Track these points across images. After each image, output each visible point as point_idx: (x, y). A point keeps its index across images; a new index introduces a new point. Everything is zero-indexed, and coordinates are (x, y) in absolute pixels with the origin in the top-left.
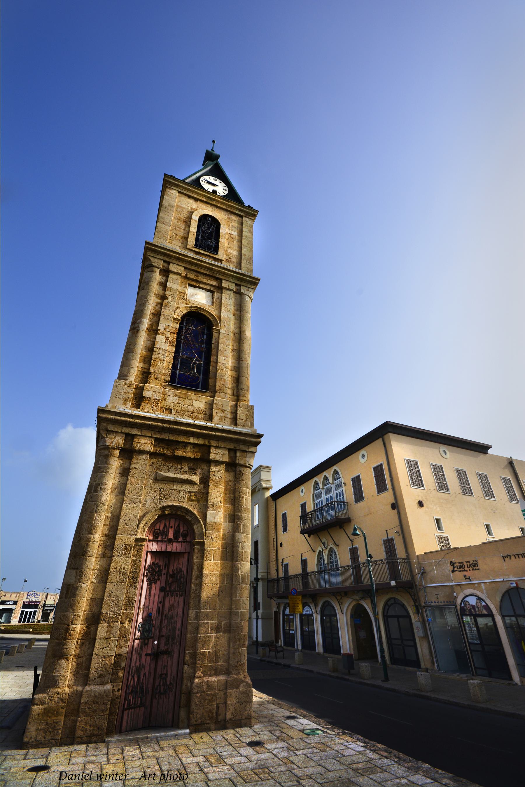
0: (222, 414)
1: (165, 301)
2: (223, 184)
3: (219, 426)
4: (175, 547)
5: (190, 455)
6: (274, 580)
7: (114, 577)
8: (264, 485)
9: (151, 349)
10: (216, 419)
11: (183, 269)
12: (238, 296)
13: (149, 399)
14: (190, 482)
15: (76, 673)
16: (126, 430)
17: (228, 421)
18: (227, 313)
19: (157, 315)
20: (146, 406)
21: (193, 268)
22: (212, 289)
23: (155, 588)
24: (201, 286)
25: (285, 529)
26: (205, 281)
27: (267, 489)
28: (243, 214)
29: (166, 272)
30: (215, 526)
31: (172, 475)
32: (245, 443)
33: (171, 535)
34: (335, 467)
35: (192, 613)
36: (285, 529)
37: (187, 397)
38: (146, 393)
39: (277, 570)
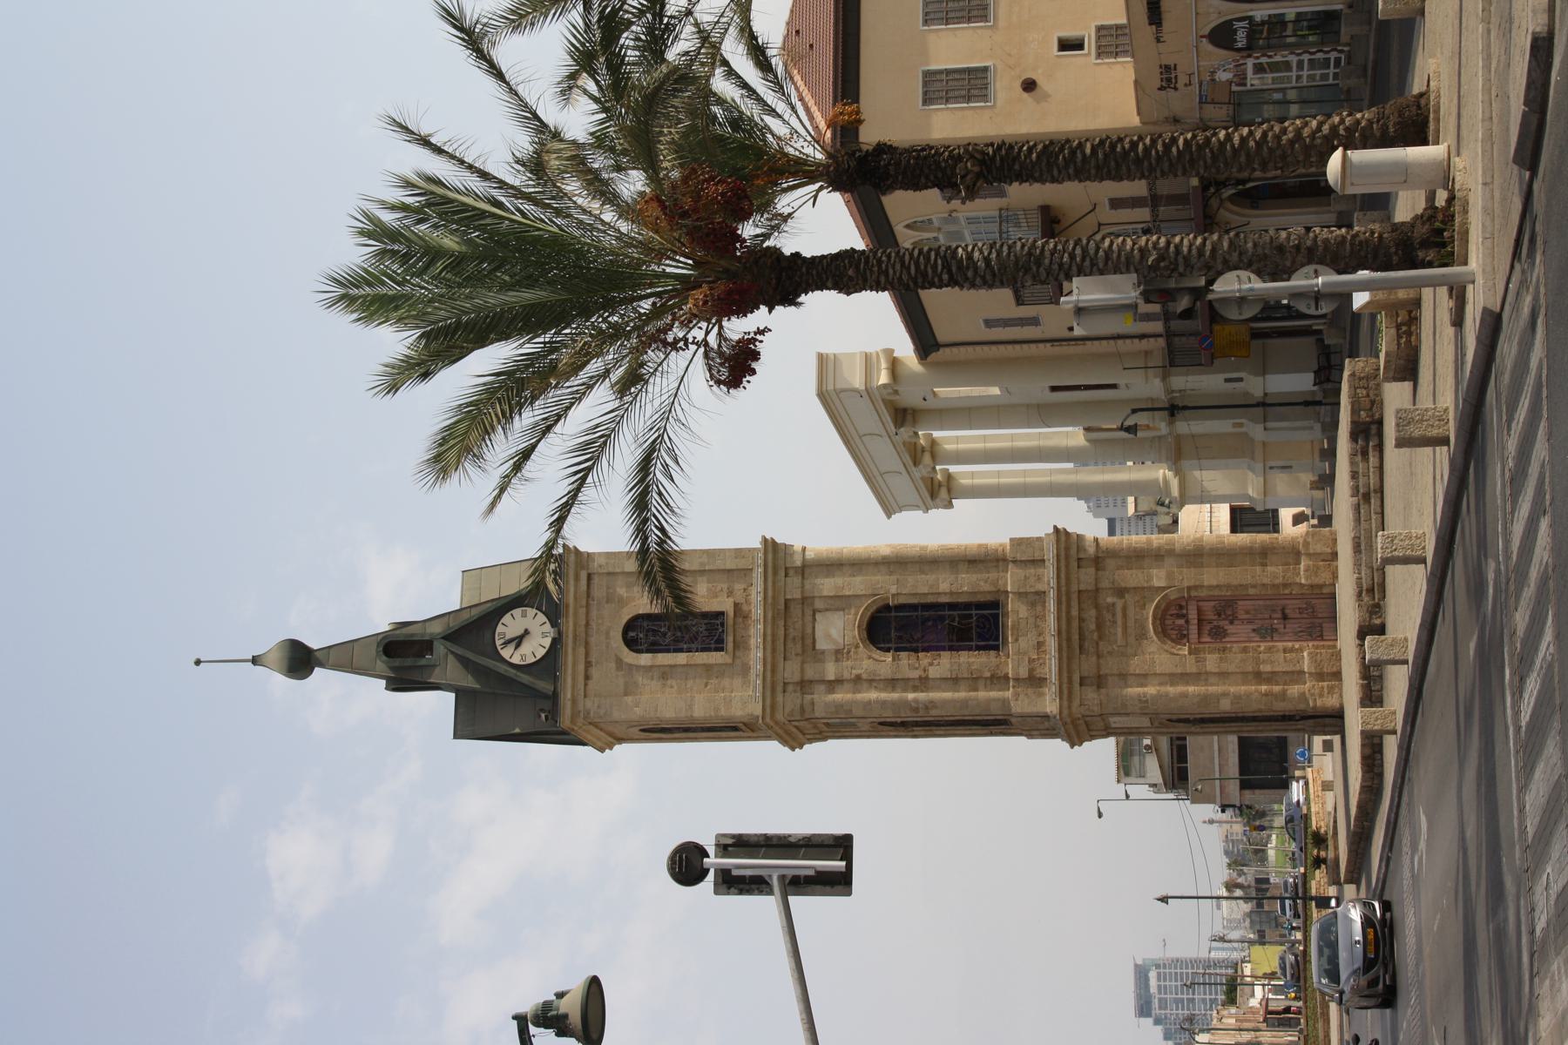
0: (1032, 580)
1: (864, 676)
2: (507, 619)
3: (1053, 583)
4: (1193, 615)
5: (1093, 612)
6: (1169, 344)
7: (1225, 667)
8: (884, 378)
9: (954, 681)
10: (1040, 587)
11: (788, 663)
12: (807, 571)
13: (1031, 671)
14: (1124, 609)
15: (1296, 682)
16: (1076, 685)
17: (1040, 571)
18: (857, 584)
19: (892, 683)
20: (1039, 673)
21: (780, 647)
22: (809, 612)
23: (1231, 629)
24: (809, 631)
25: (1034, 321)
26: (799, 625)
27: (894, 364)
28: (584, 575)
29: (804, 685)
30: (1170, 576)
31: (1120, 630)
32: (1067, 549)
33: (1181, 622)
34: (899, 229)
35: (1252, 591)
36: (1034, 321)
37: (1016, 627)
38: (1023, 673)
39: (1142, 337)
